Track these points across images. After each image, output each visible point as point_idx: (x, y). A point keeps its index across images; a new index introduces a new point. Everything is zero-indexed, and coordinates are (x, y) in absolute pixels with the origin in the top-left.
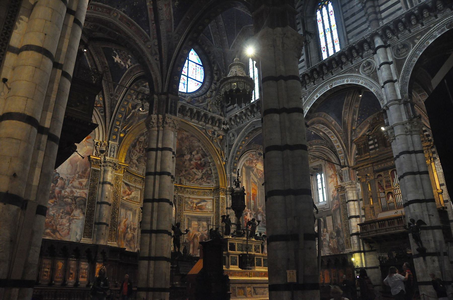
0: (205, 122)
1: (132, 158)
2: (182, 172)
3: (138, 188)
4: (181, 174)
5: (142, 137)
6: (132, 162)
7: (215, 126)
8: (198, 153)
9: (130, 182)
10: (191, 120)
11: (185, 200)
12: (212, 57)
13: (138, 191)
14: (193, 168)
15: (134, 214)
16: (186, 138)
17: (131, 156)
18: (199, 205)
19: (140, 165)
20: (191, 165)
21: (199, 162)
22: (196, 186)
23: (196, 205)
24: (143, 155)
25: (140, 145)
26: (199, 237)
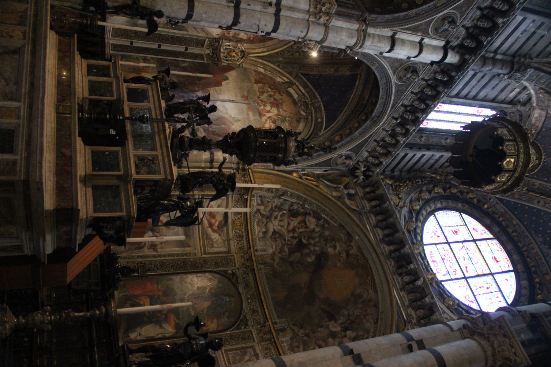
1: (273, 218)
3: (229, 245)
4: (296, 329)
5: (313, 220)
6: (267, 223)
9: (233, 222)
10: (401, 290)
11: (248, 347)
13: (225, 247)
19: (270, 240)
24: (288, 240)
25: (300, 226)
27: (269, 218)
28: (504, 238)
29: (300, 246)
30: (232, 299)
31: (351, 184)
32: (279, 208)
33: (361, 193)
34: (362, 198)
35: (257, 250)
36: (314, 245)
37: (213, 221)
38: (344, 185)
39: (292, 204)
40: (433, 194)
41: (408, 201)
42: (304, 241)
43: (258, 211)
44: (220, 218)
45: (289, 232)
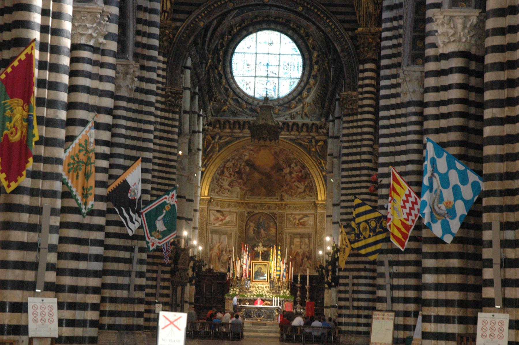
0: (297, 131)
2: (282, 186)
3: (233, 212)
4: (282, 189)
5: (229, 163)
7: (311, 131)
8: (296, 165)
12: (310, 41)
14: (294, 182)
15: (230, 237)
16: (279, 153)
17: (220, 183)
18: (302, 220)
20: (292, 178)
21: (300, 174)
22: (297, 200)
23: (299, 221)
26: (300, 254)
27: (221, 187)
28: (258, 27)
29: (239, 173)
30: (262, 217)
31: (211, 133)
32: (218, 180)
33: (217, 130)
34: (222, 132)
35: (237, 197)
36: (241, 165)
37: (220, 219)
38: (211, 139)
39: (218, 173)
40: (221, 72)
41: (226, 98)
42: (237, 170)
43: (217, 193)
44: (218, 215)
45: (230, 177)
